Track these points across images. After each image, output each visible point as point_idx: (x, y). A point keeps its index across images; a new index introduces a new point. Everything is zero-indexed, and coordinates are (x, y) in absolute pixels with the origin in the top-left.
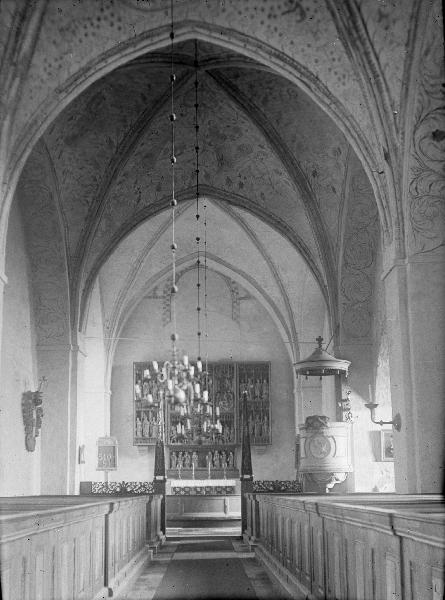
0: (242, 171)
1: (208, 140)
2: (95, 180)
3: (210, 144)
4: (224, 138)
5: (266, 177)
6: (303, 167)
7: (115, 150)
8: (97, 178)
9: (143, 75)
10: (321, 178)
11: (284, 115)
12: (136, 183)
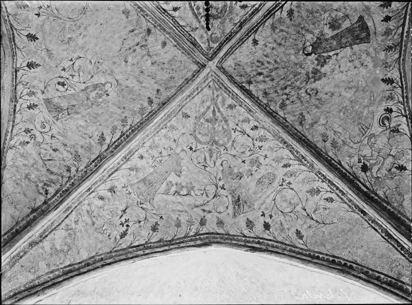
0: (266, 209)
1: (221, 184)
2: (69, 170)
3: (223, 188)
4: (240, 176)
5: (299, 208)
6: (347, 167)
7: (105, 147)
8: (73, 169)
9: (153, 81)
10: (375, 169)
11: (307, 117)
12: (124, 211)
